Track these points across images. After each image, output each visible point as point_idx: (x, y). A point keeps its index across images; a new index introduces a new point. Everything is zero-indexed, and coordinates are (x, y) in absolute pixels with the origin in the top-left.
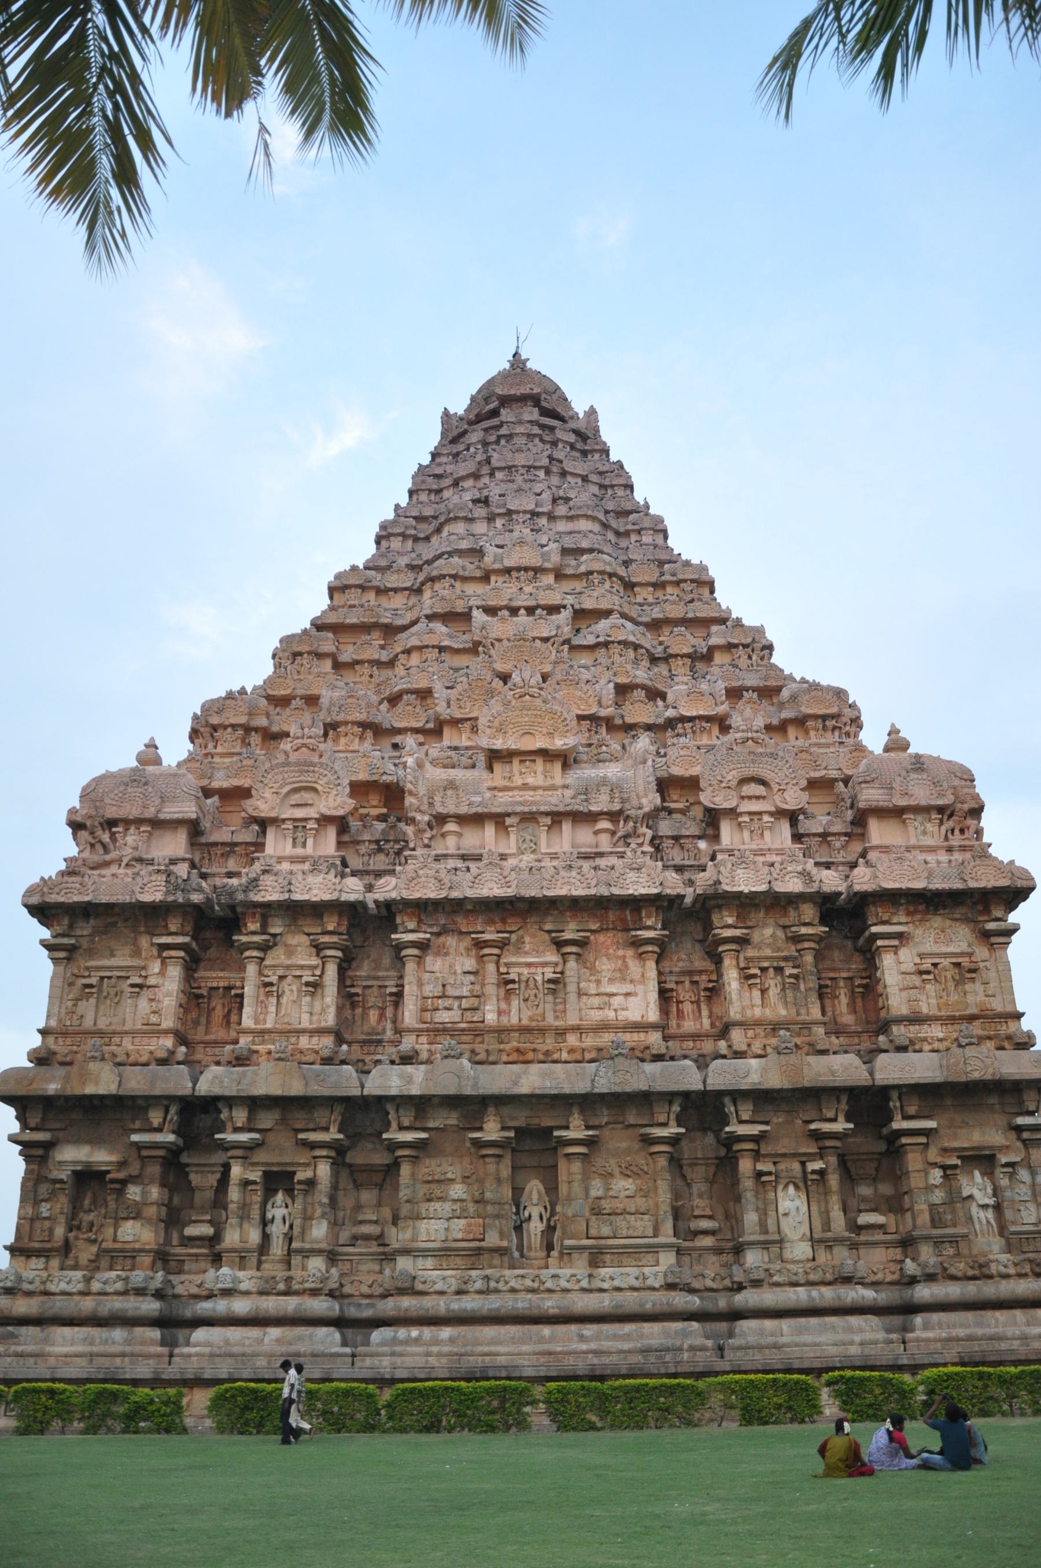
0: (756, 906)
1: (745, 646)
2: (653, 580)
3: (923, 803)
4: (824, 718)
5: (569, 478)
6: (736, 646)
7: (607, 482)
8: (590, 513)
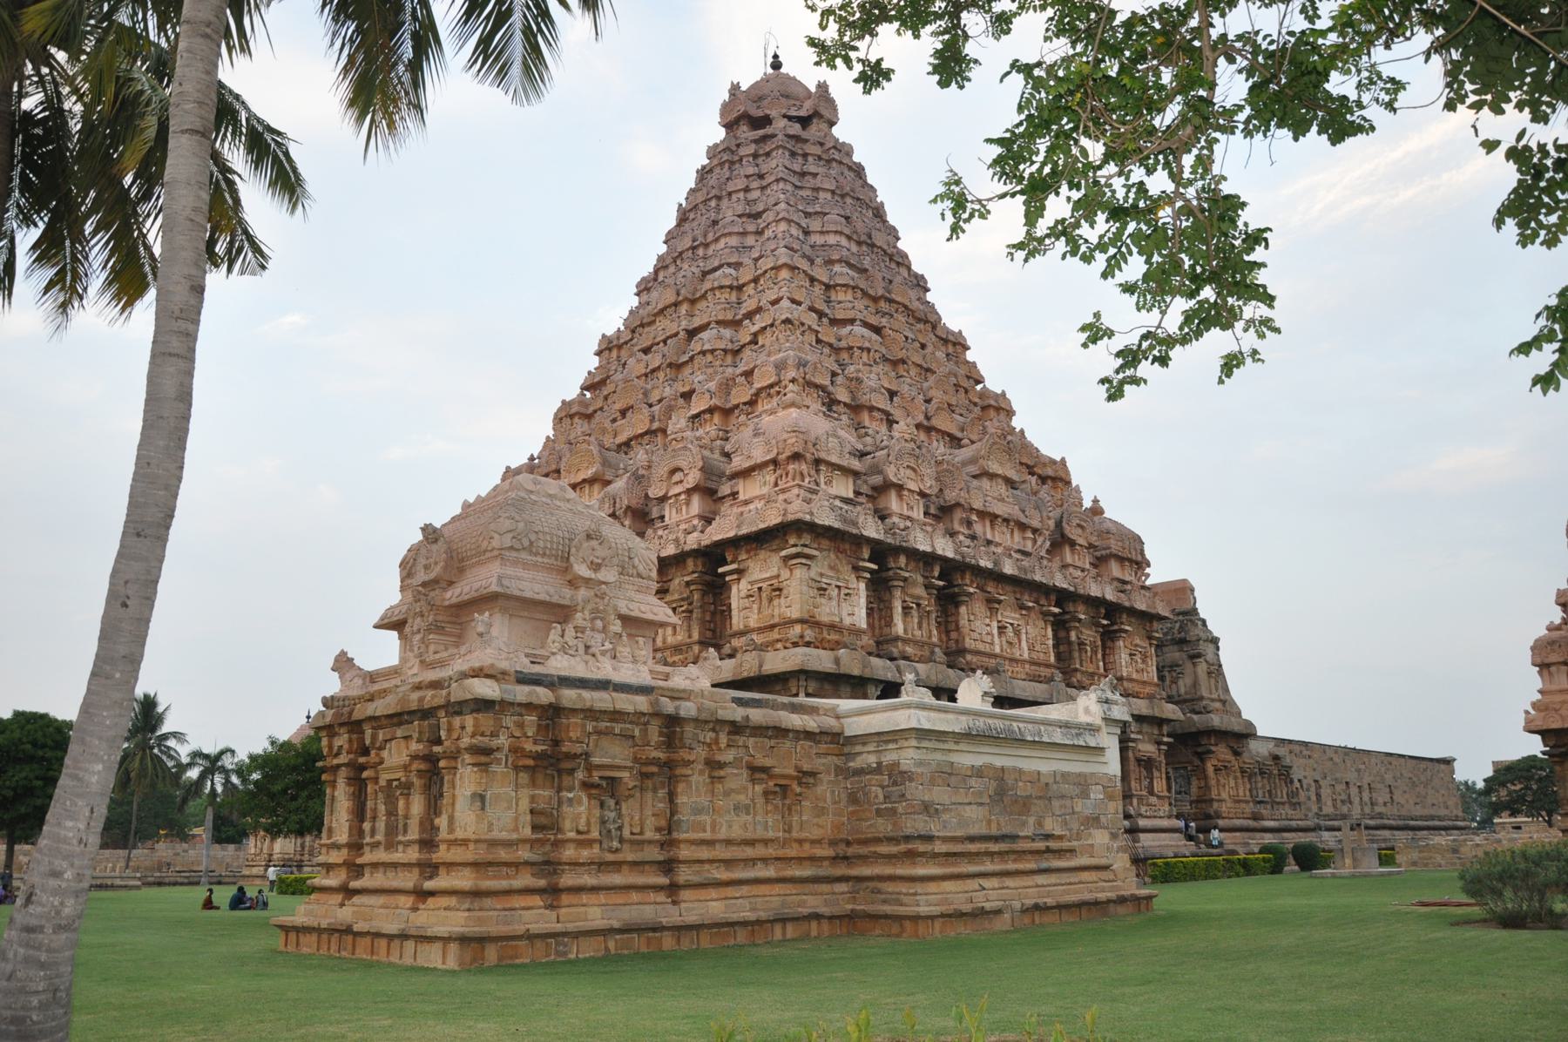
0: (670, 564)
1: (772, 325)
2: (751, 277)
3: (759, 461)
4: (771, 386)
5: (734, 197)
6: (765, 328)
7: (764, 183)
8: (726, 231)
